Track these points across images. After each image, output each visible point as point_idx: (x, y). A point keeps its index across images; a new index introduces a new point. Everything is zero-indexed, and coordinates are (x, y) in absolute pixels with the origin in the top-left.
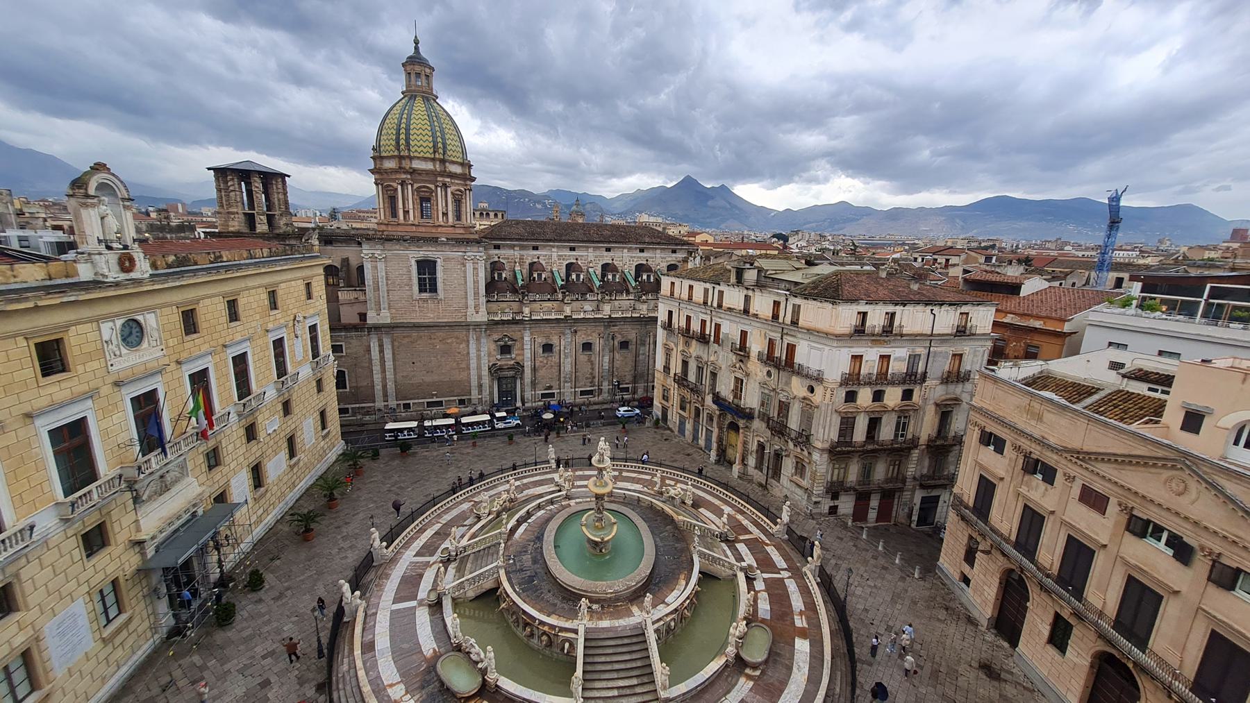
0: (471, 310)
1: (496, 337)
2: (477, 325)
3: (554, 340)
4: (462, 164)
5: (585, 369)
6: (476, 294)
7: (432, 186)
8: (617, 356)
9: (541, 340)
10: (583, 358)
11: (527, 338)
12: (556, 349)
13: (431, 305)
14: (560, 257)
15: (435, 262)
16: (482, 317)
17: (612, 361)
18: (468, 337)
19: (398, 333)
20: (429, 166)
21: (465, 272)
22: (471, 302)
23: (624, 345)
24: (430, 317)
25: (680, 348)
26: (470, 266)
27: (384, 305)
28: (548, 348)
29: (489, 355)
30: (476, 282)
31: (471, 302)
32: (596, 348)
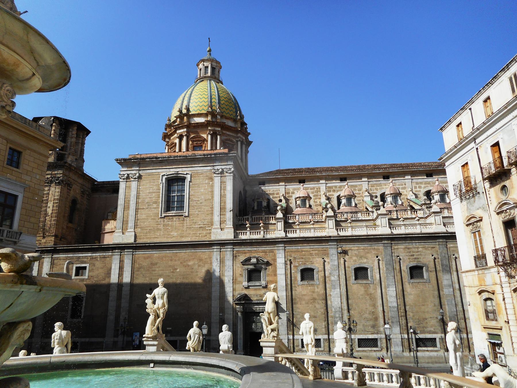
0: (217, 224)
1: (242, 258)
2: (222, 244)
3: (316, 264)
4: (235, 121)
5: (361, 308)
6: (222, 209)
7: (204, 136)
8: (408, 288)
9: (299, 265)
10: (357, 288)
11: (280, 260)
12: (318, 276)
13: (176, 222)
14: (329, 189)
15: (183, 179)
16: (228, 234)
17: (402, 294)
18: (211, 258)
19: (140, 253)
20: (201, 120)
21: (212, 186)
22: (216, 218)
23: (416, 271)
24: (174, 237)
25: (494, 205)
26: (217, 180)
27: (131, 224)
28: (307, 274)
29: (234, 281)
30: (222, 197)
31: (216, 218)
32: (374, 274)
